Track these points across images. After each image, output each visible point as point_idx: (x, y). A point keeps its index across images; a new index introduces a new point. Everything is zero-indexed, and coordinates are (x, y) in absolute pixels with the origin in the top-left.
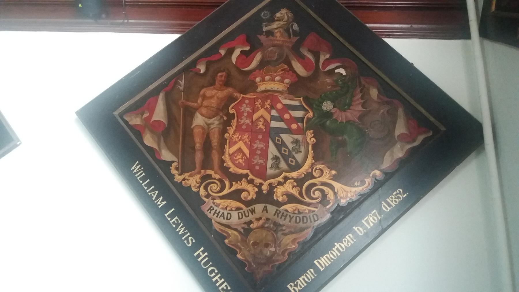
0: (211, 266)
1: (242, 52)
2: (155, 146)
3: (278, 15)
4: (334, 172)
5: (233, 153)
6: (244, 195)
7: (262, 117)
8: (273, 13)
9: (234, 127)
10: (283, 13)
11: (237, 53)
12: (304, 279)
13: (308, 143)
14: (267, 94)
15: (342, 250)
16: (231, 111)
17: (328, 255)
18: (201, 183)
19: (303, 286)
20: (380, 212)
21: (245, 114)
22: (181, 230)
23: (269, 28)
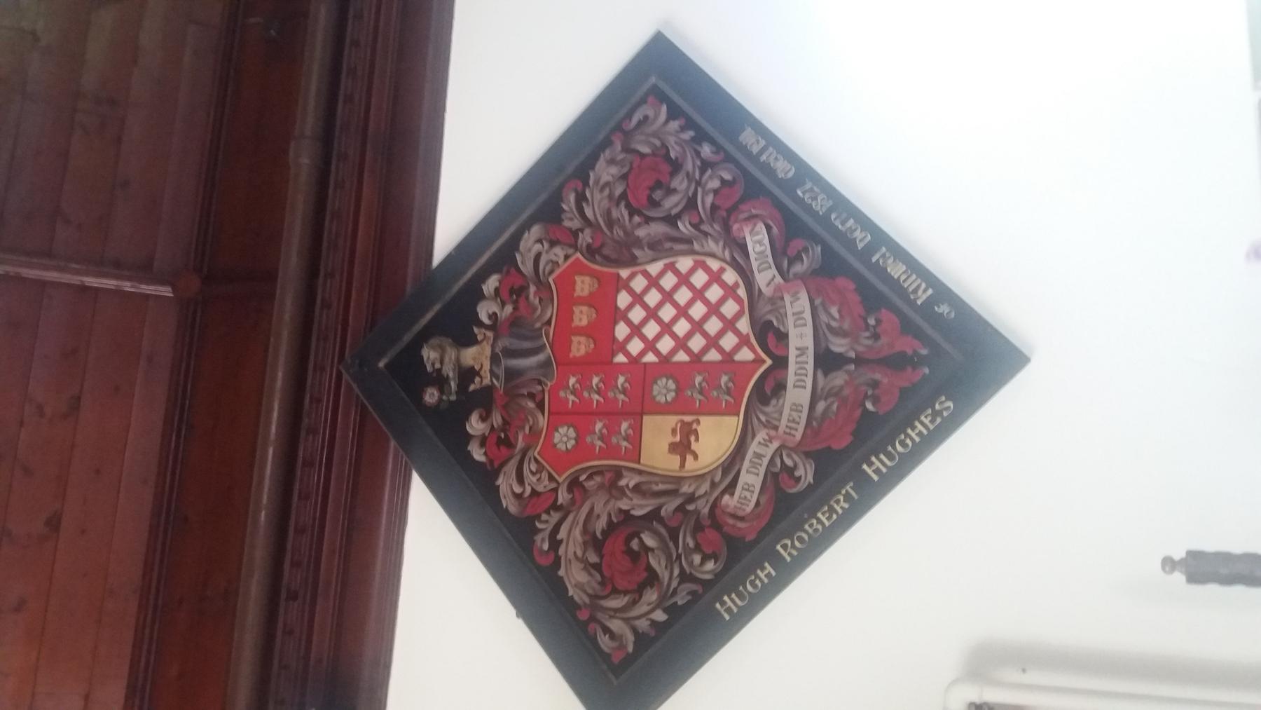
12: (919, 286)
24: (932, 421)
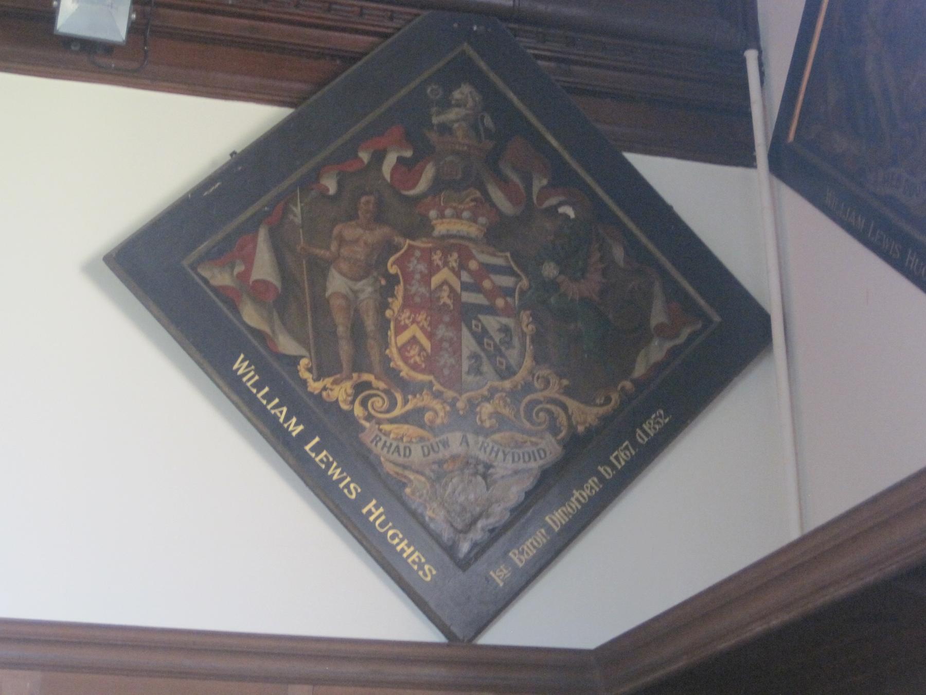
0: (390, 528)
1: (400, 160)
2: (265, 327)
3: (457, 95)
4: (565, 382)
5: (404, 346)
6: (428, 416)
7: (445, 282)
8: (449, 91)
9: (400, 299)
10: (464, 92)
11: (391, 160)
12: (532, 543)
13: (524, 334)
14: (452, 241)
15: (583, 501)
16: (393, 270)
17: (564, 509)
18: (355, 396)
19: (531, 554)
20: (635, 444)
21: (418, 276)
22: (335, 473)
23: (442, 118)
24: (414, 562)
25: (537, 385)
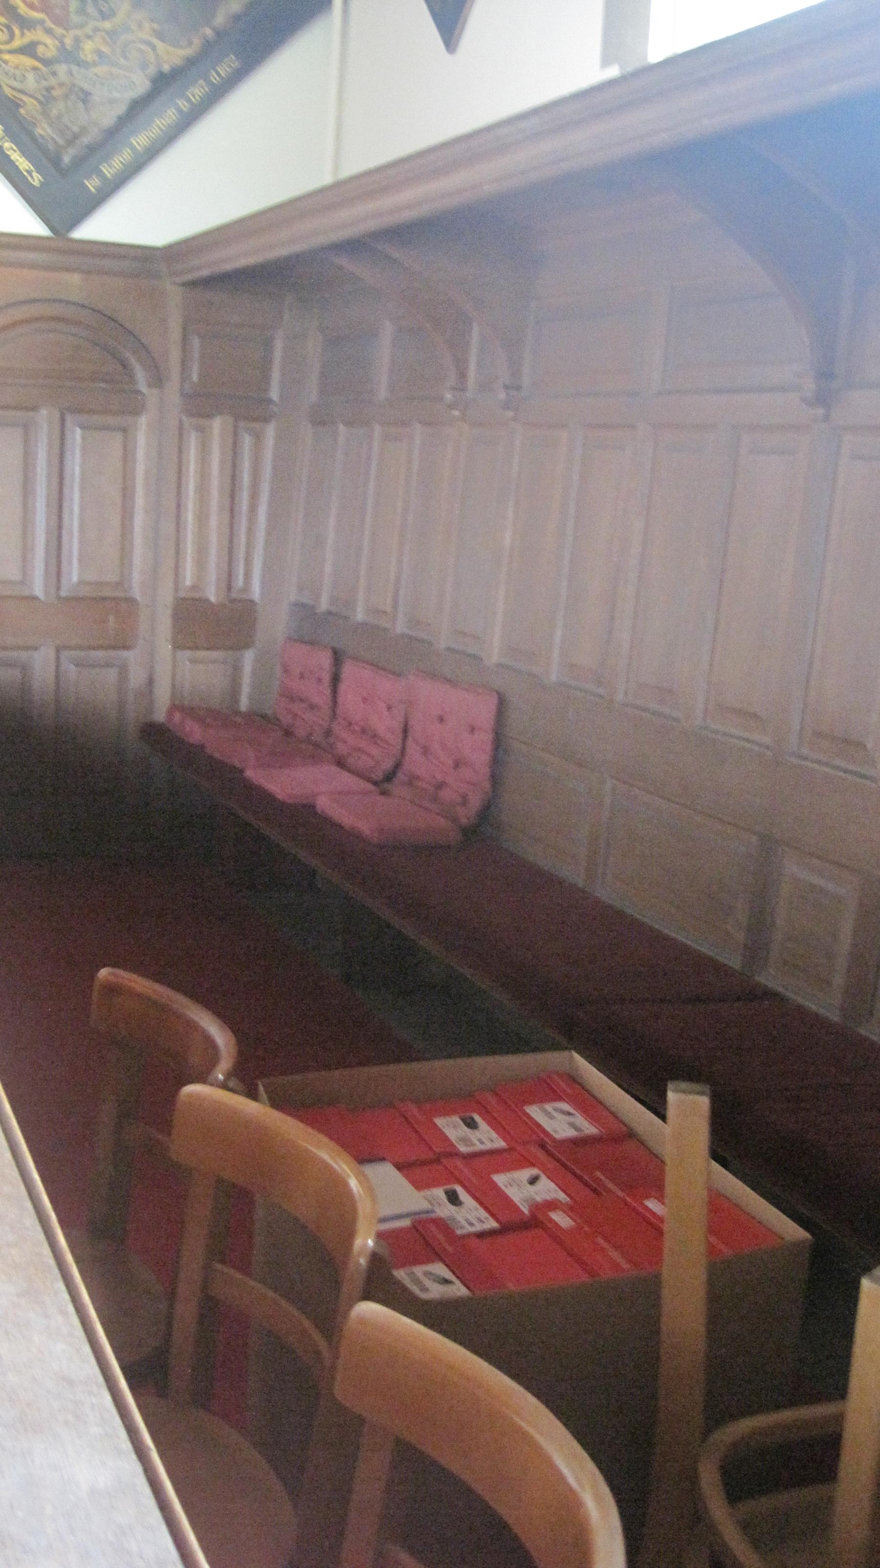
15: (163, 128)
25: (134, 27)
